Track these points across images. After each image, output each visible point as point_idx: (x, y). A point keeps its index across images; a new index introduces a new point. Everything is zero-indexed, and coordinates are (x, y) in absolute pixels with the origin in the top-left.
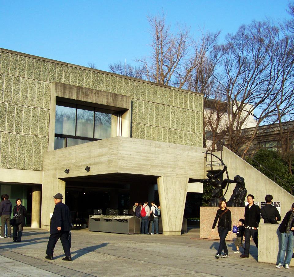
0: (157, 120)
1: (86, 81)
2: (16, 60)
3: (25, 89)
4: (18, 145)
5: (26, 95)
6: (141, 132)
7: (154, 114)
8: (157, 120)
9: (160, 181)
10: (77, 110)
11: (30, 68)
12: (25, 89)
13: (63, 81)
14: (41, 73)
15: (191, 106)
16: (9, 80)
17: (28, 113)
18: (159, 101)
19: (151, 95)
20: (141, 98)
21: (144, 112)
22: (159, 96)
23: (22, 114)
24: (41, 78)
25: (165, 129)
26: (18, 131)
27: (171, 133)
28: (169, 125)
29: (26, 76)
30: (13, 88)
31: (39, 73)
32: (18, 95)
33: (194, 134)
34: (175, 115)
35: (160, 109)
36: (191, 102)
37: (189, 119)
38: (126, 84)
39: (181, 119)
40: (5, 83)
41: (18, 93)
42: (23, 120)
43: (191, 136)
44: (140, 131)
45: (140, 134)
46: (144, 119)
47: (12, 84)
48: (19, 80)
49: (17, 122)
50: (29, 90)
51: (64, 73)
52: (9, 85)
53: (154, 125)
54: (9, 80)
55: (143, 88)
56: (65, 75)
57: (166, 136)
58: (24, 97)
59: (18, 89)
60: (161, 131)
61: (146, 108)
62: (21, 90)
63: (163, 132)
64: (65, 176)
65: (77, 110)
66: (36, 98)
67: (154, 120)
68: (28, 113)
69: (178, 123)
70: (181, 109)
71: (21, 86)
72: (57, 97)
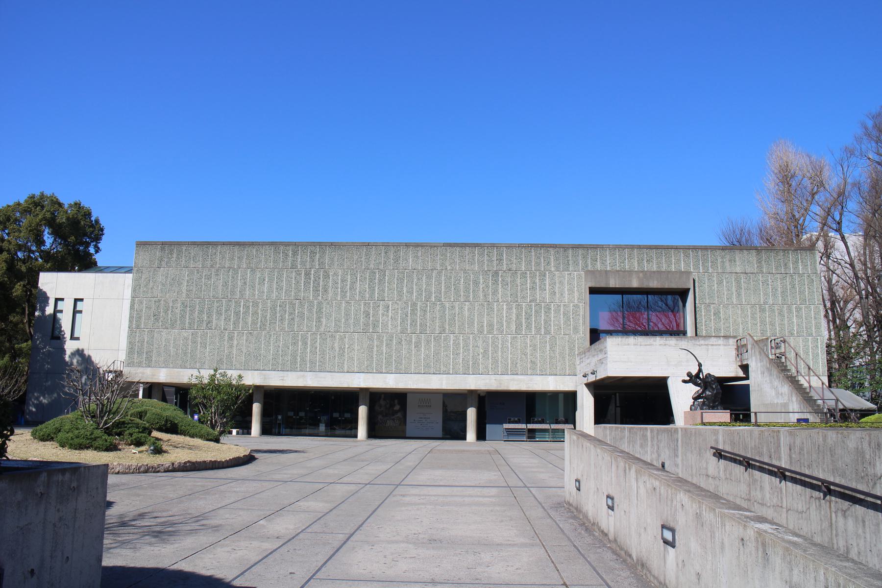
0: (739, 295)
1: (629, 261)
2: (540, 253)
3: (553, 284)
4: (548, 348)
5: (554, 291)
6: (715, 314)
7: (734, 288)
8: (739, 295)
9: (670, 383)
10: (622, 296)
11: (557, 259)
12: (553, 284)
13: (599, 266)
14: (571, 262)
15: (796, 268)
16: (533, 277)
17: (557, 311)
18: (738, 270)
19: (727, 264)
20: (710, 270)
21: (717, 287)
22: (738, 263)
23: (550, 313)
24: (571, 269)
25: (753, 306)
26: (547, 332)
27: (762, 310)
28: (760, 300)
29: (553, 269)
30: (538, 285)
31: (568, 263)
32: (545, 292)
33: (806, 307)
34: (768, 284)
35: (742, 281)
36: (796, 262)
37: (793, 287)
38: (687, 256)
39: (779, 289)
40: (528, 281)
41: (545, 290)
42: (552, 319)
43: (798, 310)
44: (712, 313)
45: (712, 318)
46: (718, 297)
47: (537, 281)
48: (545, 275)
49: (546, 322)
50: (557, 285)
51: (598, 257)
52: (534, 283)
53: (735, 303)
54: (533, 277)
55: (713, 256)
56: (601, 259)
57: (756, 316)
58: (551, 294)
59: (545, 285)
60: (747, 309)
61: (720, 282)
62: (547, 286)
63: (749, 310)
64: (592, 378)
65: (622, 296)
66: (567, 292)
67: (734, 297)
68: (557, 311)
69: (774, 295)
70: (778, 276)
71: (547, 282)
72: (589, 288)
